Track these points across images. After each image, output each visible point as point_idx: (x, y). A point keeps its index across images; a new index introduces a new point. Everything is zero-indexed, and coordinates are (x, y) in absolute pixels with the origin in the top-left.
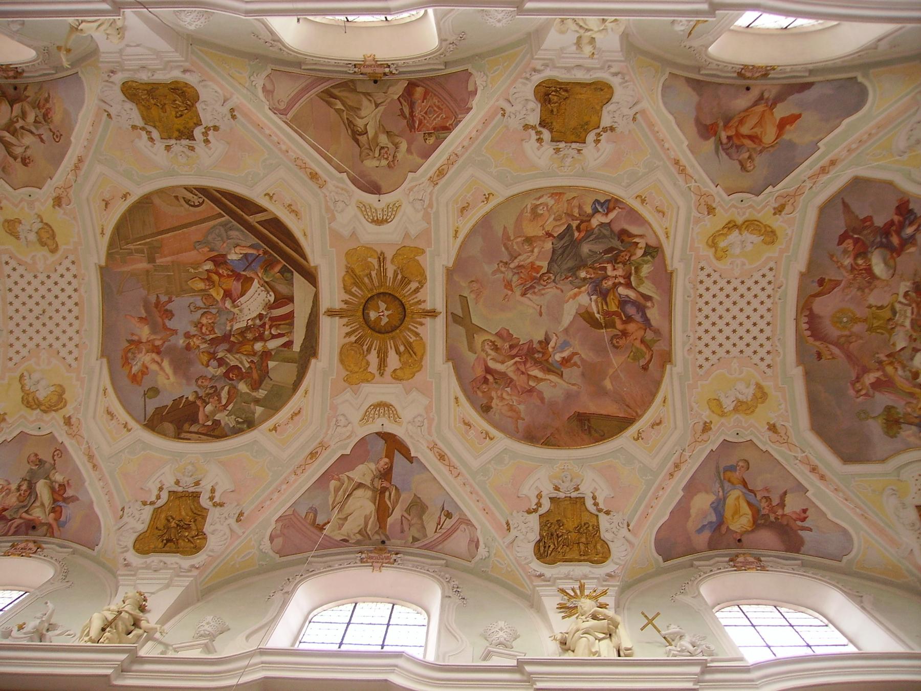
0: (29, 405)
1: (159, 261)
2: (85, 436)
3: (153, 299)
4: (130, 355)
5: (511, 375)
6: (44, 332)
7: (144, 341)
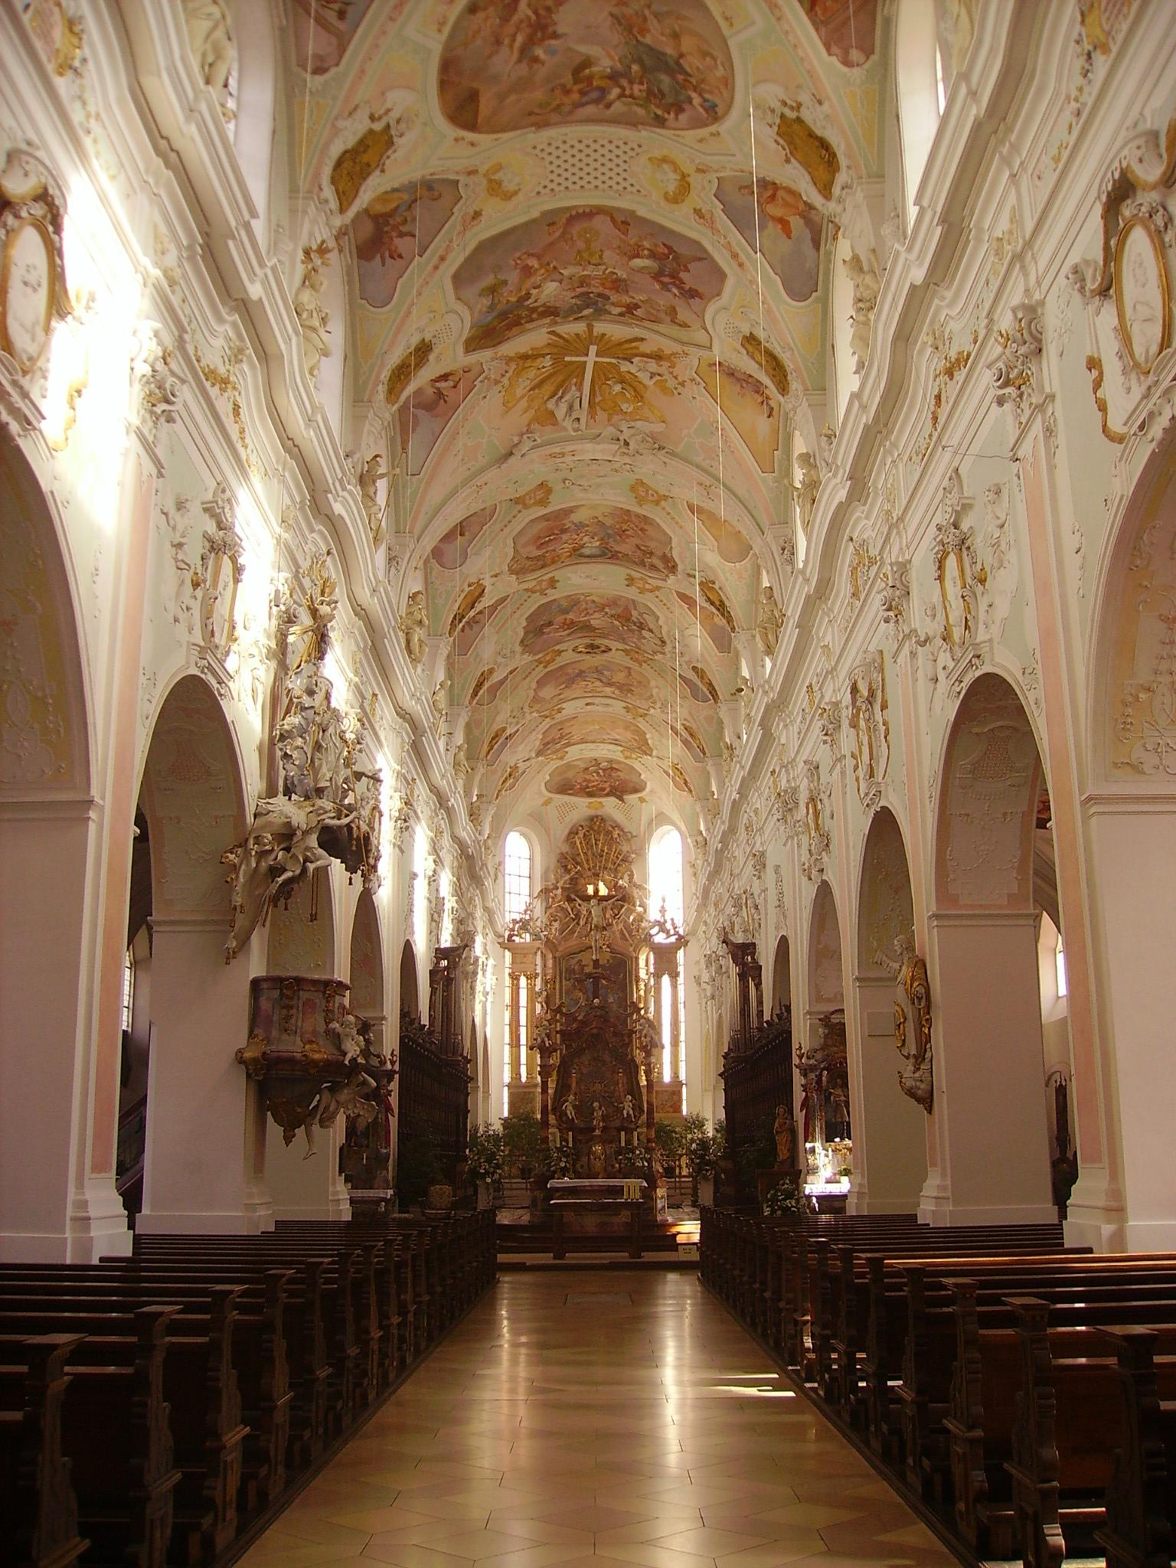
5: (515, 18)
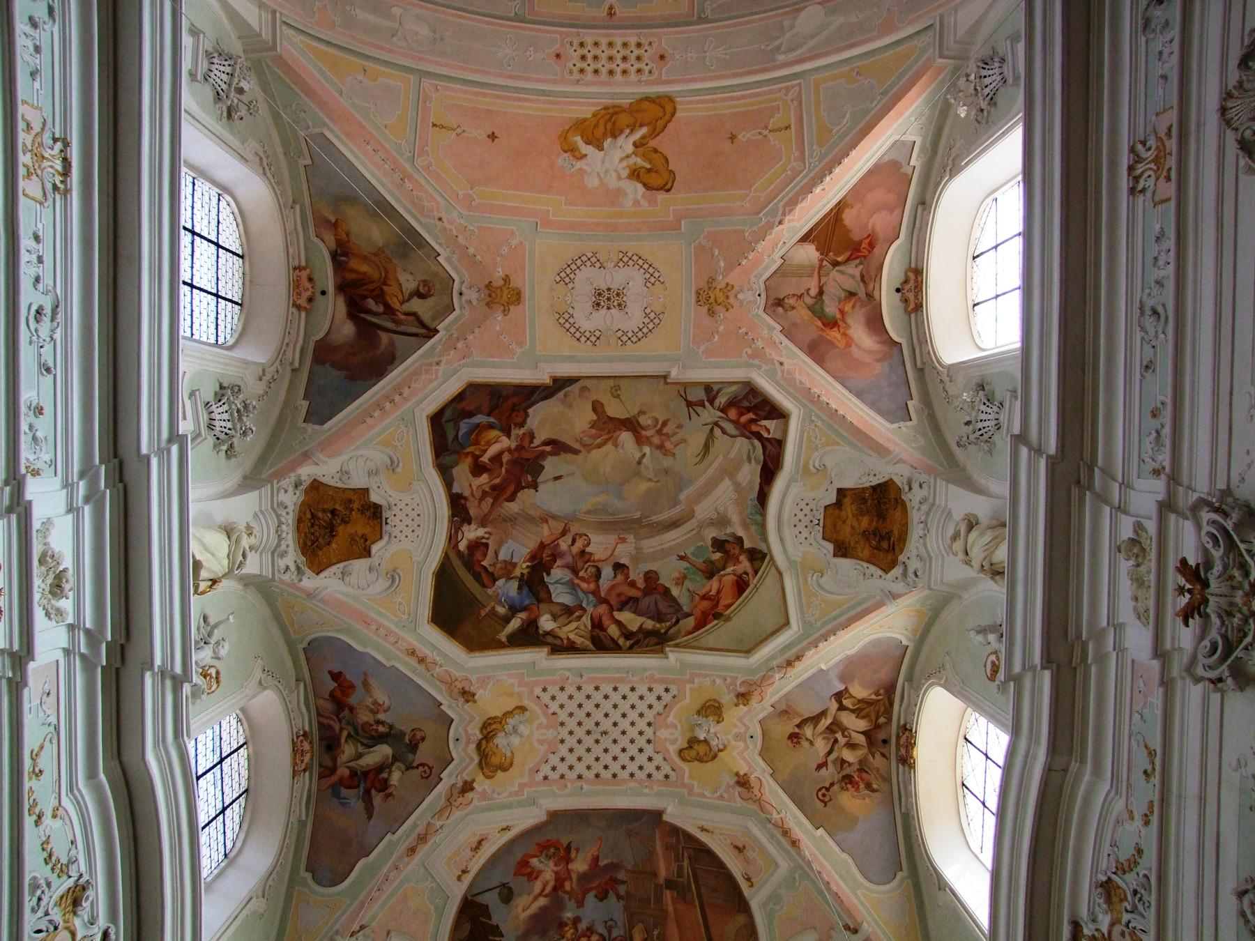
0: (485, 726)
1: (668, 894)
2: (452, 819)
3: (621, 875)
4: (552, 850)
6: (580, 733)
7: (570, 866)
